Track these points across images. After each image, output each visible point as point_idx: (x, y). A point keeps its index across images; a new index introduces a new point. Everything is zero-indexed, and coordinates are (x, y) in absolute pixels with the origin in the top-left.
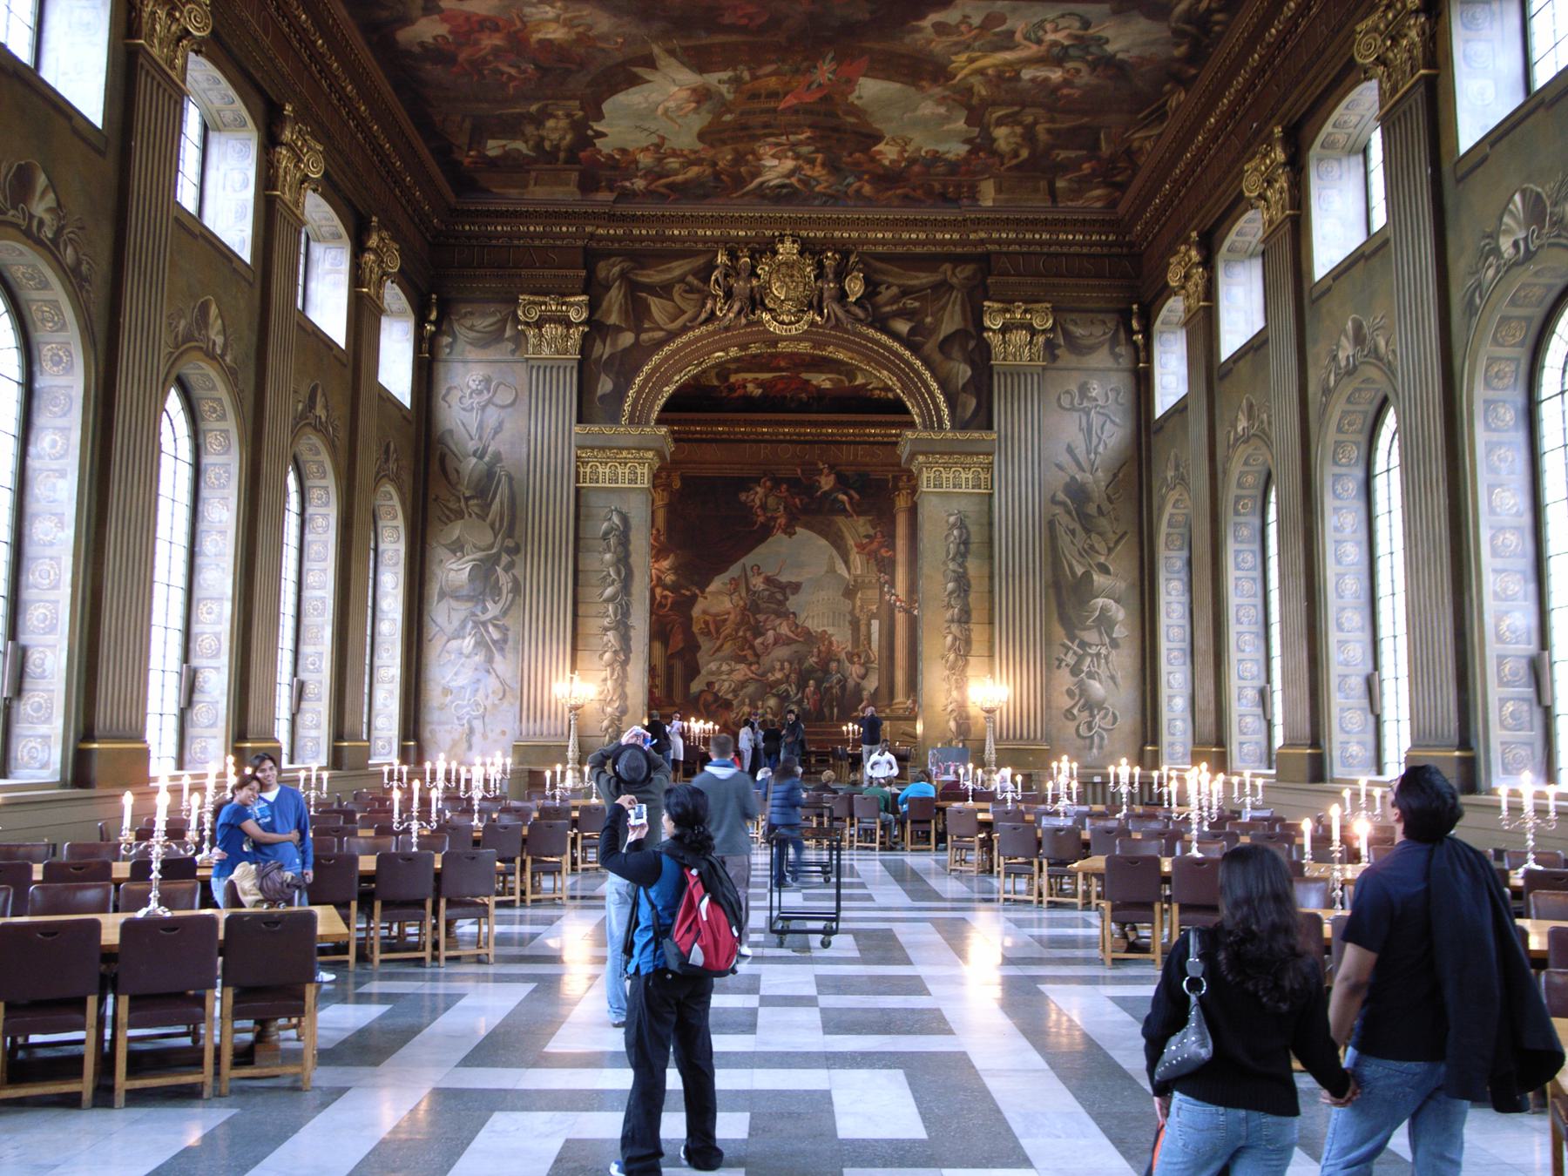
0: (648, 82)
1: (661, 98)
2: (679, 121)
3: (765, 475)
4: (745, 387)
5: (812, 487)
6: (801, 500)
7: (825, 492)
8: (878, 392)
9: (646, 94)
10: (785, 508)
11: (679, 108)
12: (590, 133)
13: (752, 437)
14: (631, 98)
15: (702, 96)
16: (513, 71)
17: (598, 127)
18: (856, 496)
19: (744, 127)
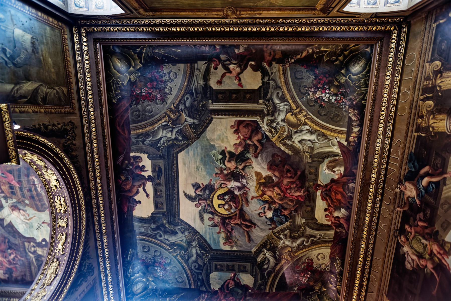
0: (10, 221)
1: (19, 219)
2: (31, 216)
3: (396, 237)
4: (338, 217)
5: (411, 204)
6: (420, 220)
7: (418, 195)
8: (351, 139)
9: (18, 224)
10: (426, 240)
11: (24, 215)
12: (44, 243)
13: (373, 228)
14: (21, 228)
15: (14, 208)
16: (12, 256)
17: (39, 240)
18: (426, 169)
19: (32, 197)
